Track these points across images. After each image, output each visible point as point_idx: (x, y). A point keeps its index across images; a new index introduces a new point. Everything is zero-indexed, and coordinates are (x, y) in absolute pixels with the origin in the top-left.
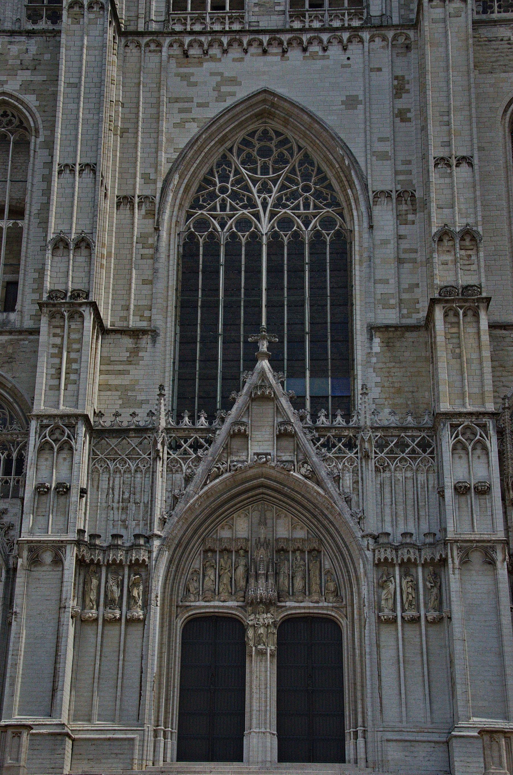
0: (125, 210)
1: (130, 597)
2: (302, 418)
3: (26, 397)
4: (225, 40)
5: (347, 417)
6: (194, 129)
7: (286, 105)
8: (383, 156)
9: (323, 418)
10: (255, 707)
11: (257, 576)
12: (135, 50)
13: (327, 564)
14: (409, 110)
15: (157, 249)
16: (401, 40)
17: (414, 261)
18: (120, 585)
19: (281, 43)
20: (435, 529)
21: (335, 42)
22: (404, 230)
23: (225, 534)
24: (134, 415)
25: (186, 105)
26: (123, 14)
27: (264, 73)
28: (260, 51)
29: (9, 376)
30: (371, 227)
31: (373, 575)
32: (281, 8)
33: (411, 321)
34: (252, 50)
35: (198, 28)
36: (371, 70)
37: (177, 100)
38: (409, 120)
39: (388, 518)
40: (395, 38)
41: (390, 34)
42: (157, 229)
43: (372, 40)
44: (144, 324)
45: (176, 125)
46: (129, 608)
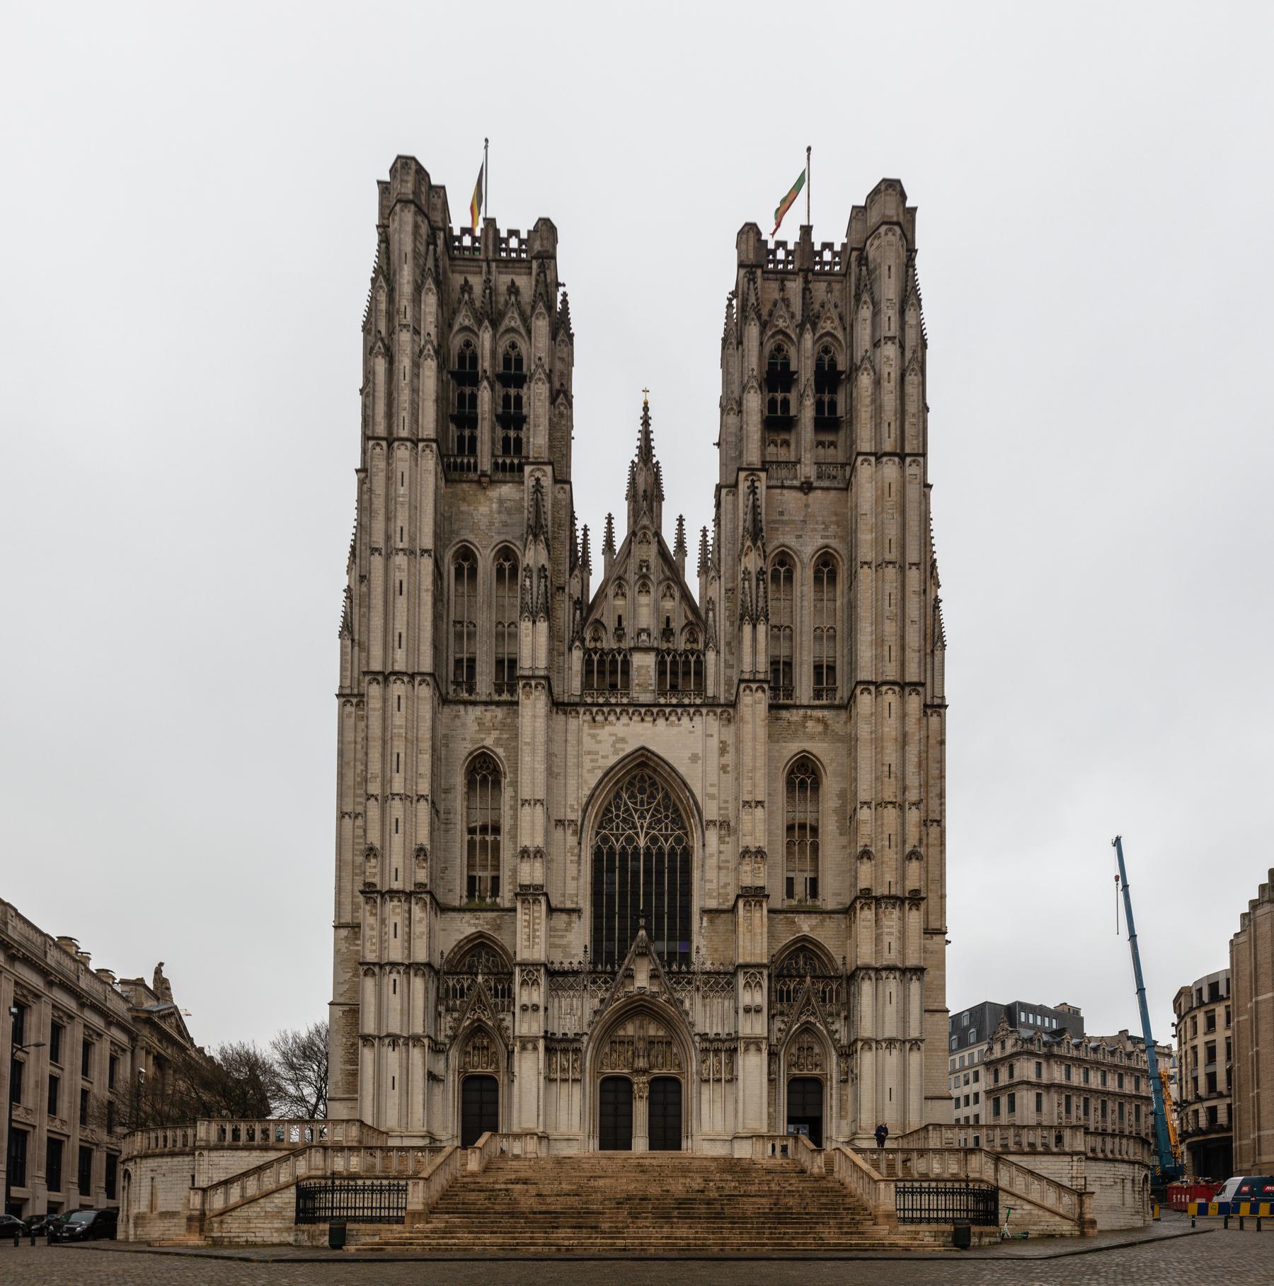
0: (560, 829)
1: (573, 1067)
2: (664, 967)
3: (511, 951)
4: (618, 710)
5: (688, 966)
6: (600, 774)
7: (656, 759)
8: (712, 797)
9: (674, 967)
10: (638, 1124)
11: (639, 1056)
12: (561, 717)
13: (675, 1050)
14: (728, 765)
15: (579, 856)
16: (725, 715)
17: (727, 868)
18: (568, 1061)
19: (652, 714)
20: (732, 1031)
21: (685, 714)
22: (723, 847)
23: (621, 1033)
24: (571, 963)
25: (595, 757)
26: (556, 690)
27: (642, 735)
28: (639, 719)
29: (499, 938)
30: (704, 845)
31: (699, 1056)
32: (652, 688)
33: (724, 907)
34: (636, 718)
35: (601, 700)
36: (707, 736)
37: (589, 753)
38: (728, 772)
39: (708, 1025)
40: (721, 714)
41: (719, 711)
42: (580, 843)
43: (707, 714)
44: (574, 906)
45: (589, 771)
46: (573, 1073)
